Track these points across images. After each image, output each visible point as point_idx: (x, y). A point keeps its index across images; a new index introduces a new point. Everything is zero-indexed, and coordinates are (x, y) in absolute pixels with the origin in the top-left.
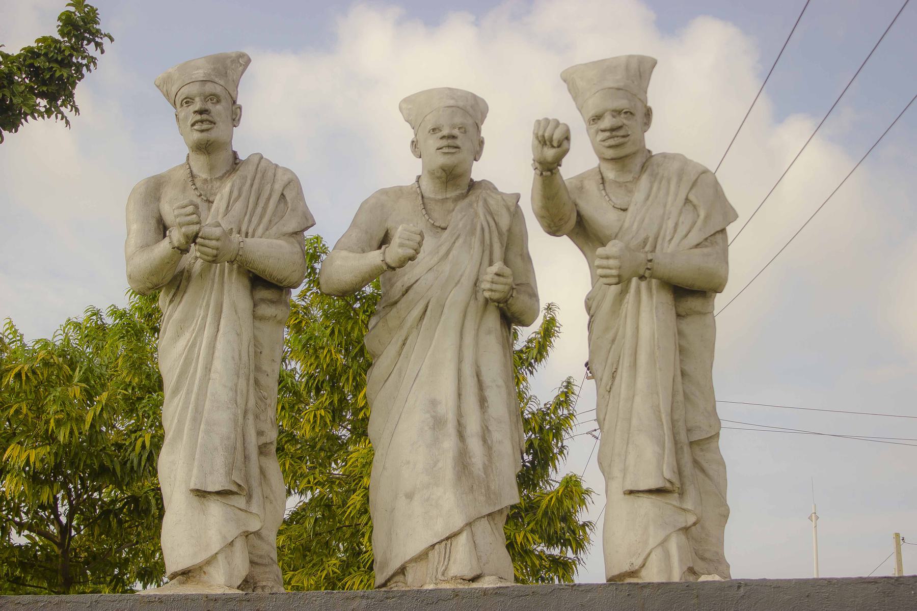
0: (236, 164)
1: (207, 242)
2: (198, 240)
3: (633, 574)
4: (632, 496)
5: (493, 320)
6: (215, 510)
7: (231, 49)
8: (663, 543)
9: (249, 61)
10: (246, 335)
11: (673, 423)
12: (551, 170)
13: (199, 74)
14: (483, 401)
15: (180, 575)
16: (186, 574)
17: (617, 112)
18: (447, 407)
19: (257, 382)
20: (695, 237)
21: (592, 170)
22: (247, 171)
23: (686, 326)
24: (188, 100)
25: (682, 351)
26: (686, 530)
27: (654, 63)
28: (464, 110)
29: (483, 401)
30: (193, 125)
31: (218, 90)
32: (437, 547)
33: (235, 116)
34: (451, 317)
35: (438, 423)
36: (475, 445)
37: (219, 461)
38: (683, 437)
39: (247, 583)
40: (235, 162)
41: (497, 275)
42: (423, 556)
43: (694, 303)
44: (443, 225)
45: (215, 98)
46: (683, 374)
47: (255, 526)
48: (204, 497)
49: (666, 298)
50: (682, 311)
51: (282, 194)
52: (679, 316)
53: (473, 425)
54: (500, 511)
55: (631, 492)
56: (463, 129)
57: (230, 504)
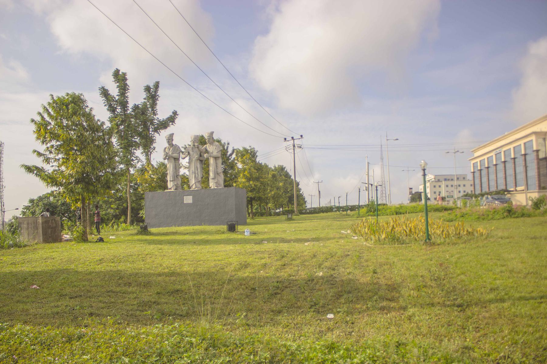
5: (199, 161)
6: (172, 182)
7: (172, 133)
8: (213, 184)
10: (174, 164)
11: (215, 172)
13: (168, 137)
14: (197, 170)
16: (170, 189)
17: (208, 139)
18: (194, 171)
19: (176, 169)
20: (216, 152)
22: (174, 146)
23: (217, 161)
25: (216, 164)
26: (216, 183)
28: (195, 138)
29: (197, 170)
31: (170, 138)
33: (172, 140)
34: (194, 161)
35: (193, 172)
36: (196, 175)
37: (171, 178)
38: (216, 173)
39: (175, 189)
40: (173, 145)
42: (192, 186)
43: (218, 159)
45: (170, 139)
46: (216, 166)
47: (176, 184)
49: (214, 159)
52: (216, 160)
53: (196, 173)
54: (199, 181)
56: (195, 140)
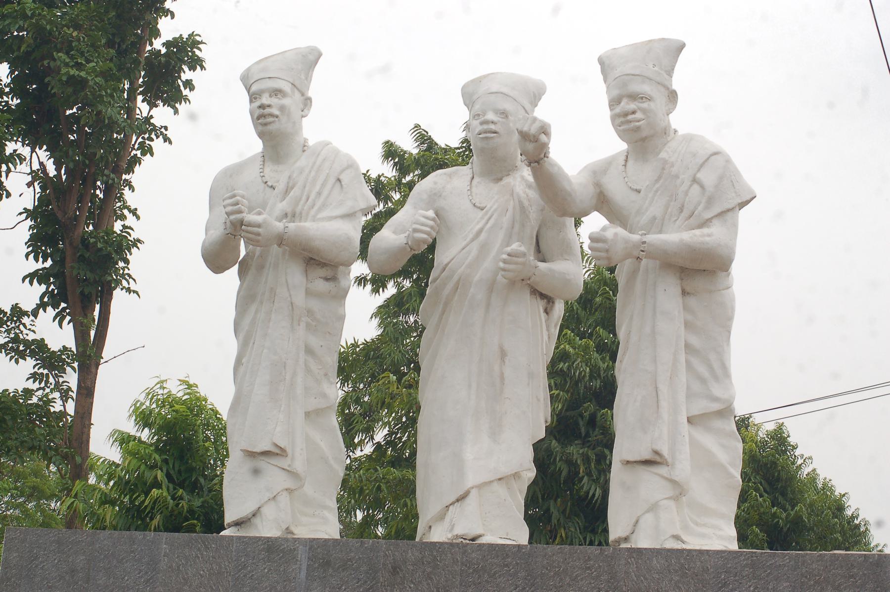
0: (304, 151)
1: (249, 228)
2: (243, 227)
3: (626, 539)
4: (629, 465)
9: (320, 55)
12: (537, 162)
15: (232, 525)
16: (238, 524)
21: (624, 150)
24: (255, 96)
27: (681, 47)
30: (258, 118)
32: (451, 507)
41: (509, 255)
44: (482, 205)
48: (254, 457)
50: (688, 289)
51: (339, 180)
52: (684, 293)
55: (628, 462)
57: (271, 463)
